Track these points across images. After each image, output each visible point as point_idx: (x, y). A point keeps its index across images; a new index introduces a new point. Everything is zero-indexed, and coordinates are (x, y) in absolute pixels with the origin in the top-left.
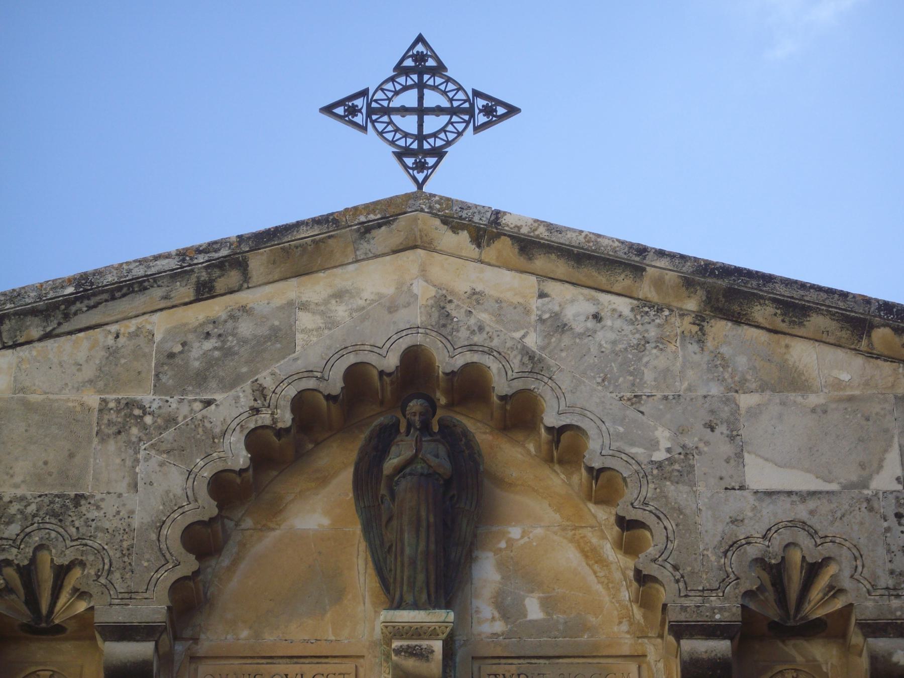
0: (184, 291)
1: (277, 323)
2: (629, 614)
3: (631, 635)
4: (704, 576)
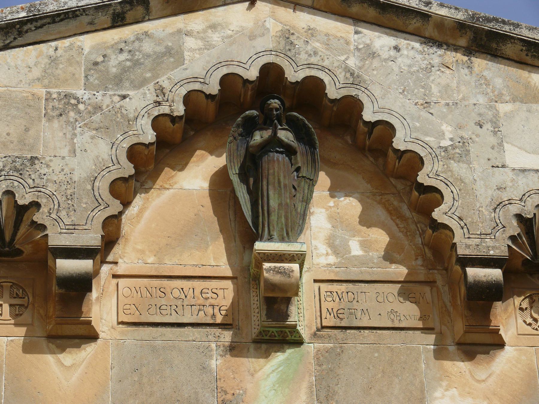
0: (104, 18)
1: (170, 44)
2: (422, 253)
3: (424, 267)
4: (481, 225)
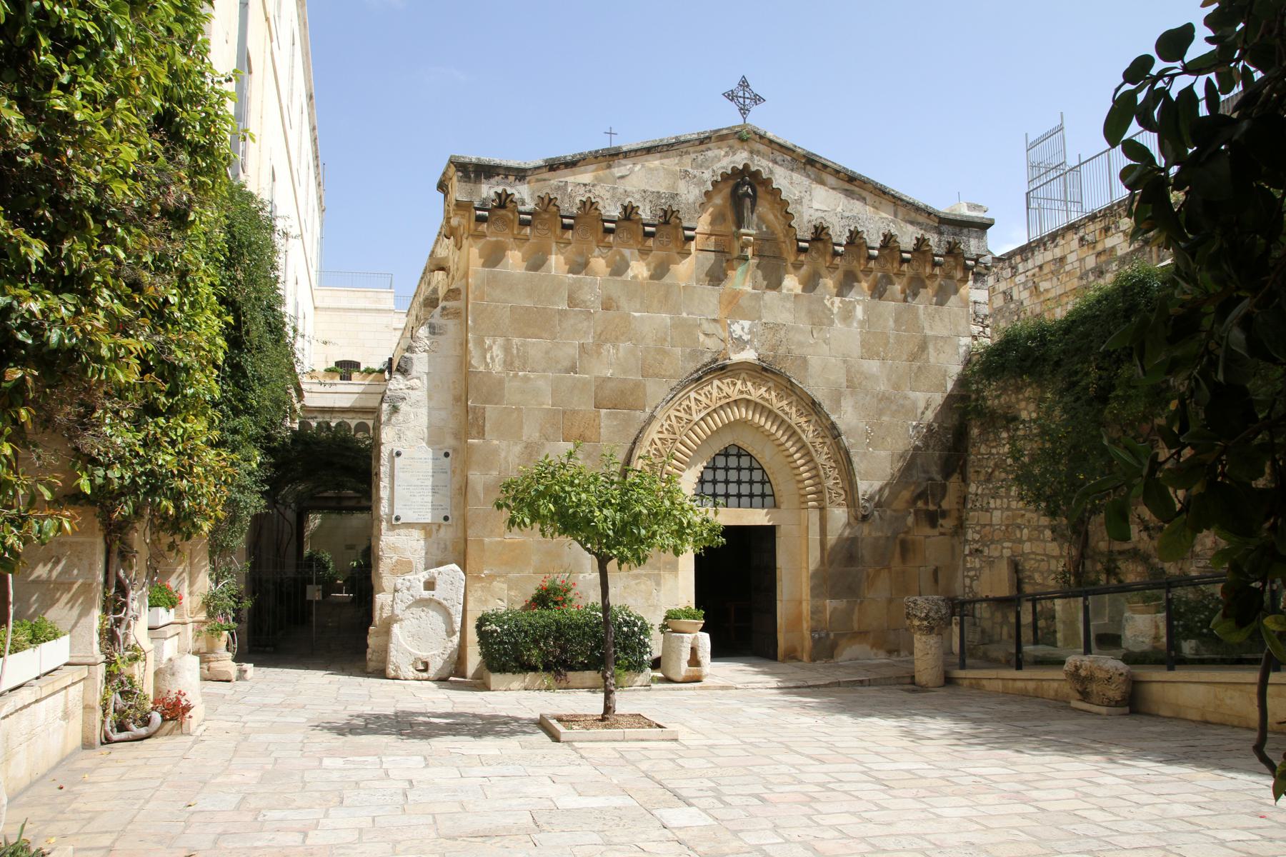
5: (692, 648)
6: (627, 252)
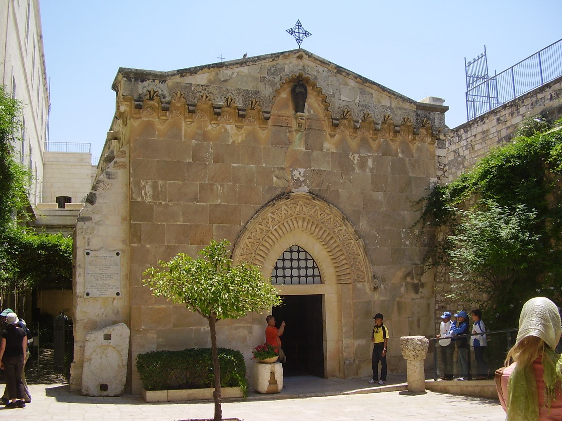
0: (271, 60)
5: (271, 373)
6: (228, 127)
